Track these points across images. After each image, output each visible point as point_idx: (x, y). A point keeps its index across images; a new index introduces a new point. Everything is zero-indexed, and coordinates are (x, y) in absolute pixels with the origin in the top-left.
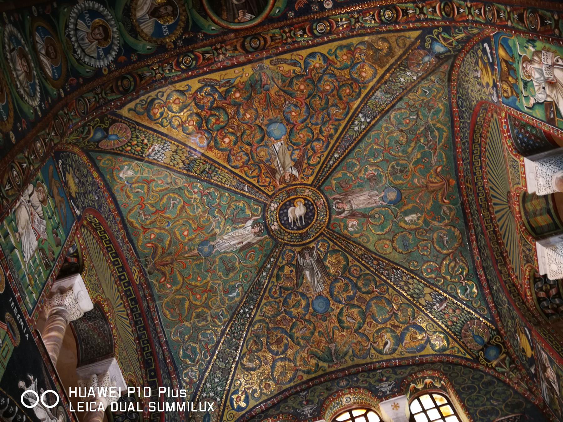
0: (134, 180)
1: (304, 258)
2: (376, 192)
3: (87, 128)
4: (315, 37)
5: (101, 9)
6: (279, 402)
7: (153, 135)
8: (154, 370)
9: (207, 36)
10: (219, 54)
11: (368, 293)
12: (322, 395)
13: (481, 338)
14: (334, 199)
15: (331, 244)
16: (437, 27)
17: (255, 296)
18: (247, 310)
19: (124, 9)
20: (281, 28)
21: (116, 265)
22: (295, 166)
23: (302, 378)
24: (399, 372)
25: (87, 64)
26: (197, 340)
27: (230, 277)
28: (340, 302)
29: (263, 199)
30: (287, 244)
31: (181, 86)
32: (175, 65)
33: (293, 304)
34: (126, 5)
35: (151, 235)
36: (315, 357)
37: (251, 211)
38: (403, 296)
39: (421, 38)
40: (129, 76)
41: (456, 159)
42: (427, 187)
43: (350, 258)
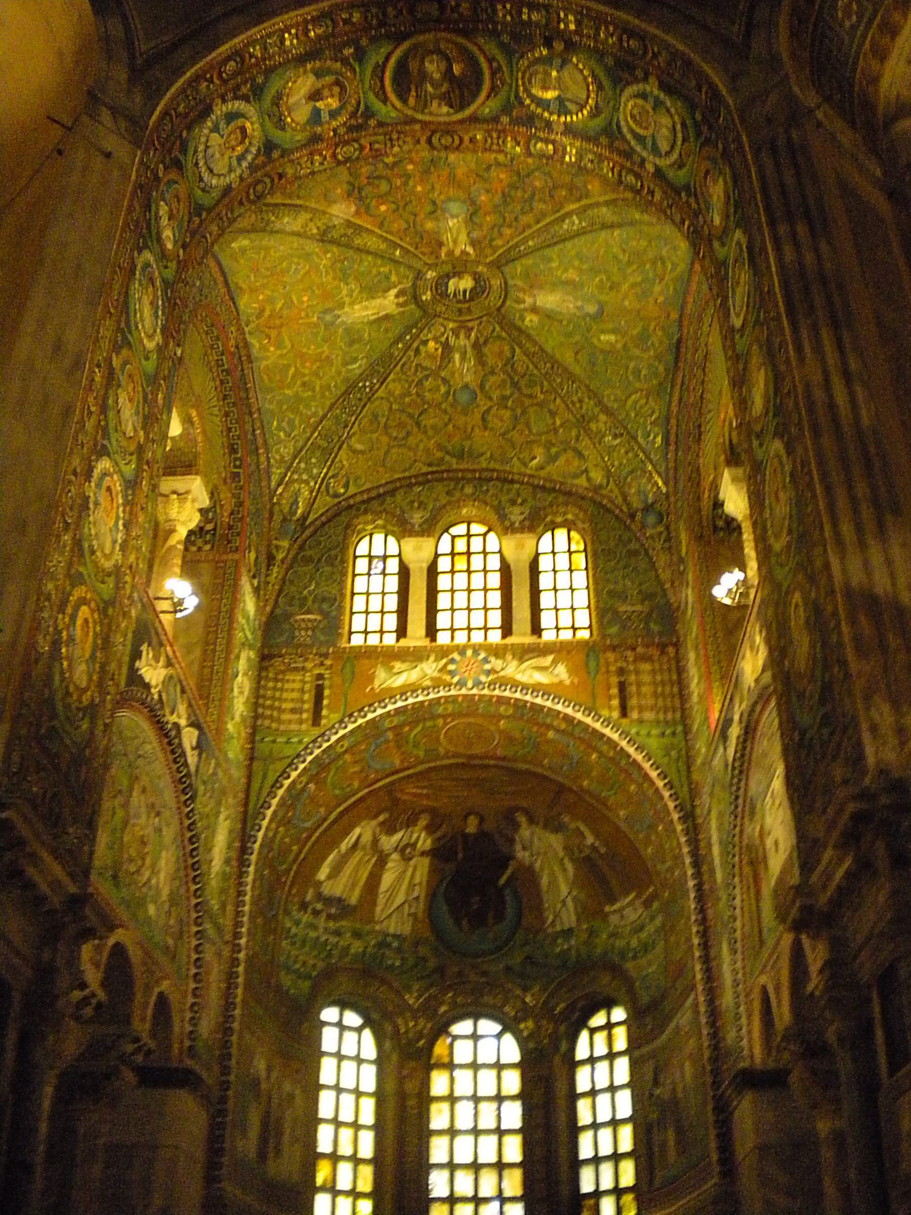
1: (457, 337)
5: (242, 106)
6: (385, 494)
8: (240, 459)
9: (381, 124)
10: (392, 146)
11: (530, 396)
13: (646, 497)
15: (498, 329)
20: (489, 132)
22: (473, 243)
29: (418, 265)
42: (639, 312)
43: (518, 350)
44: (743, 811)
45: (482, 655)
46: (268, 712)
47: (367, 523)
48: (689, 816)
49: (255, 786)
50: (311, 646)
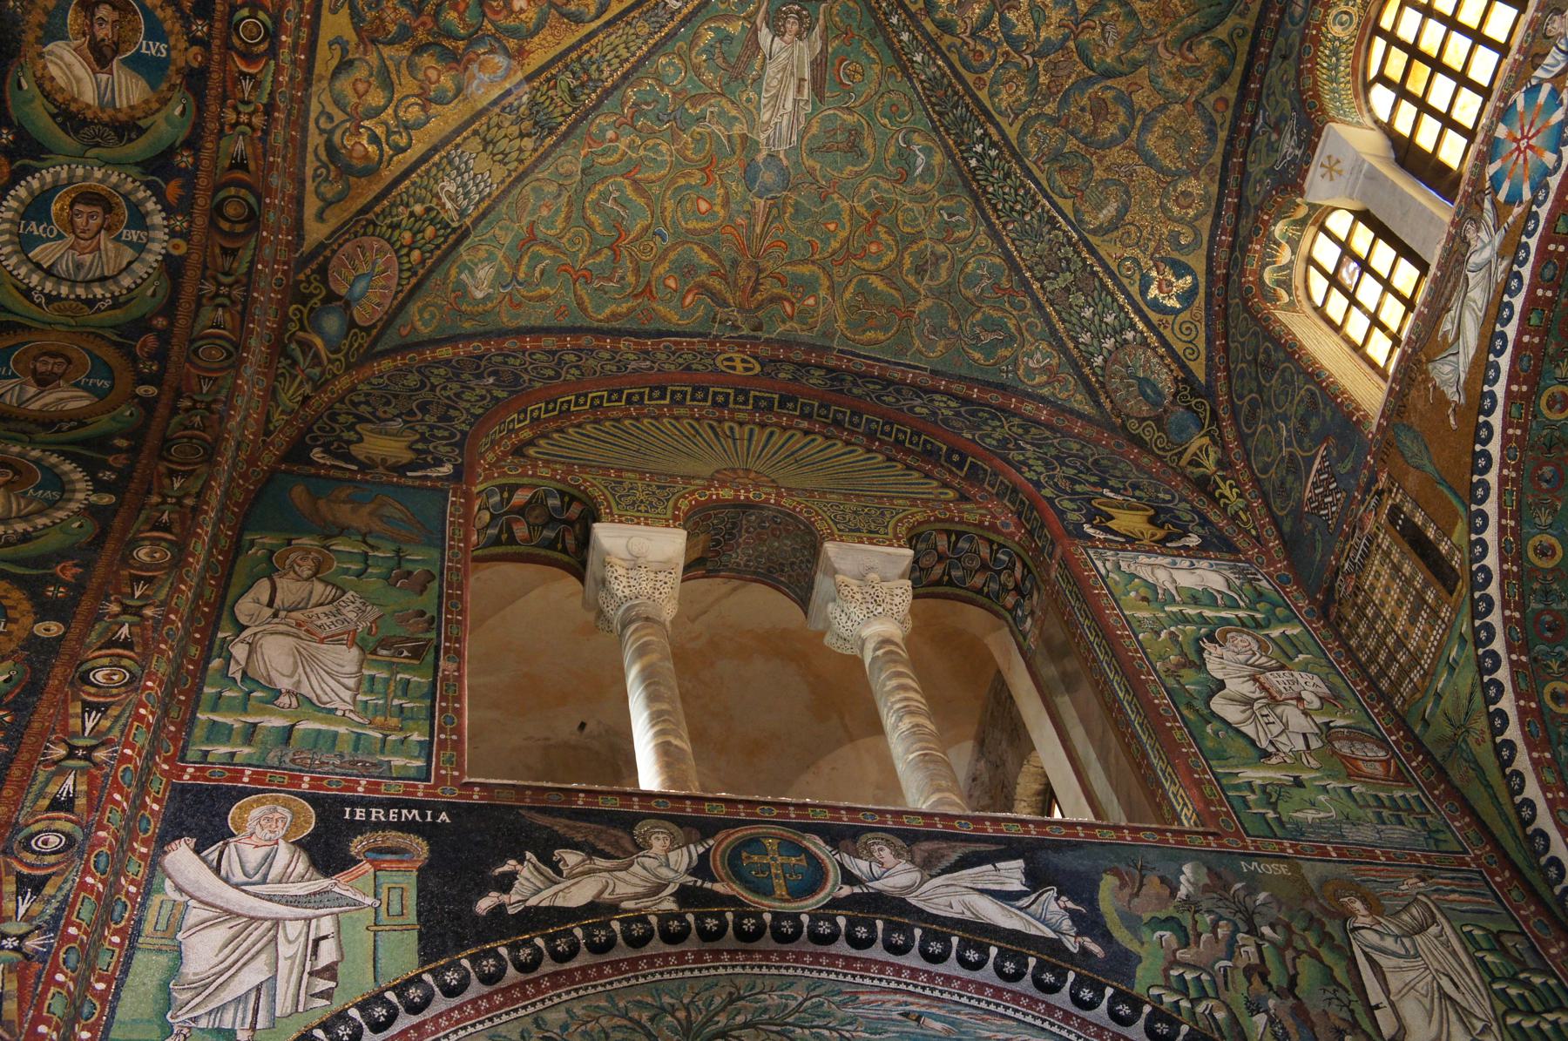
0: (506, 270)
3: (293, 346)
6: (1240, 195)
7: (414, 183)
8: (951, 451)
12: (1287, 82)
17: (958, 112)
18: (979, 148)
19: (62, 126)
21: (684, 398)
23: (1225, 101)
25: (138, 286)
26: (972, 303)
27: (871, 150)
31: (326, 58)
32: (248, 66)
33: (1031, 25)
34: (54, 116)
35: (667, 286)
36: (1196, 40)
37: (739, 18)
40: (222, 195)
45: (1519, 98)
46: (1393, 672)
47: (1267, 259)
49: (1484, 806)
50: (1350, 499)
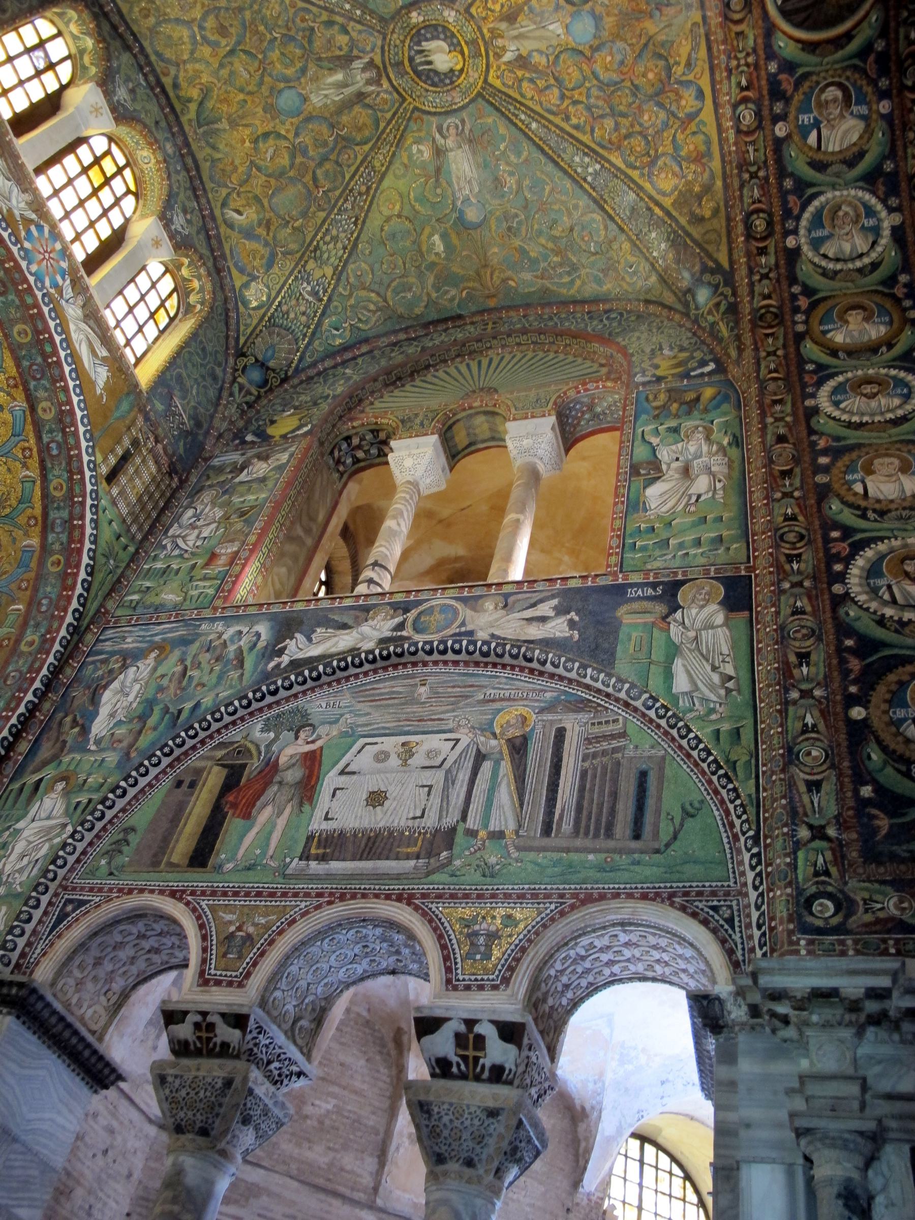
1: (364, 70)
2: (477, 190)
4: (735, 106)
11: (315, 179)
13: (272, 357)
14: (463, 122)
15: (388, 115)
16: (734, 294)
20: (755, 50)
22: (520, 57)
23: (166, 75)
24: (202, 236)
28: (297, 135)
30: (384, 39)
38: (316, 235)
39: (719, 269)
41: (528, 306)
42: (486, 266)
44: (261, 710)
45: (64, 265)
48: (77, 631)
